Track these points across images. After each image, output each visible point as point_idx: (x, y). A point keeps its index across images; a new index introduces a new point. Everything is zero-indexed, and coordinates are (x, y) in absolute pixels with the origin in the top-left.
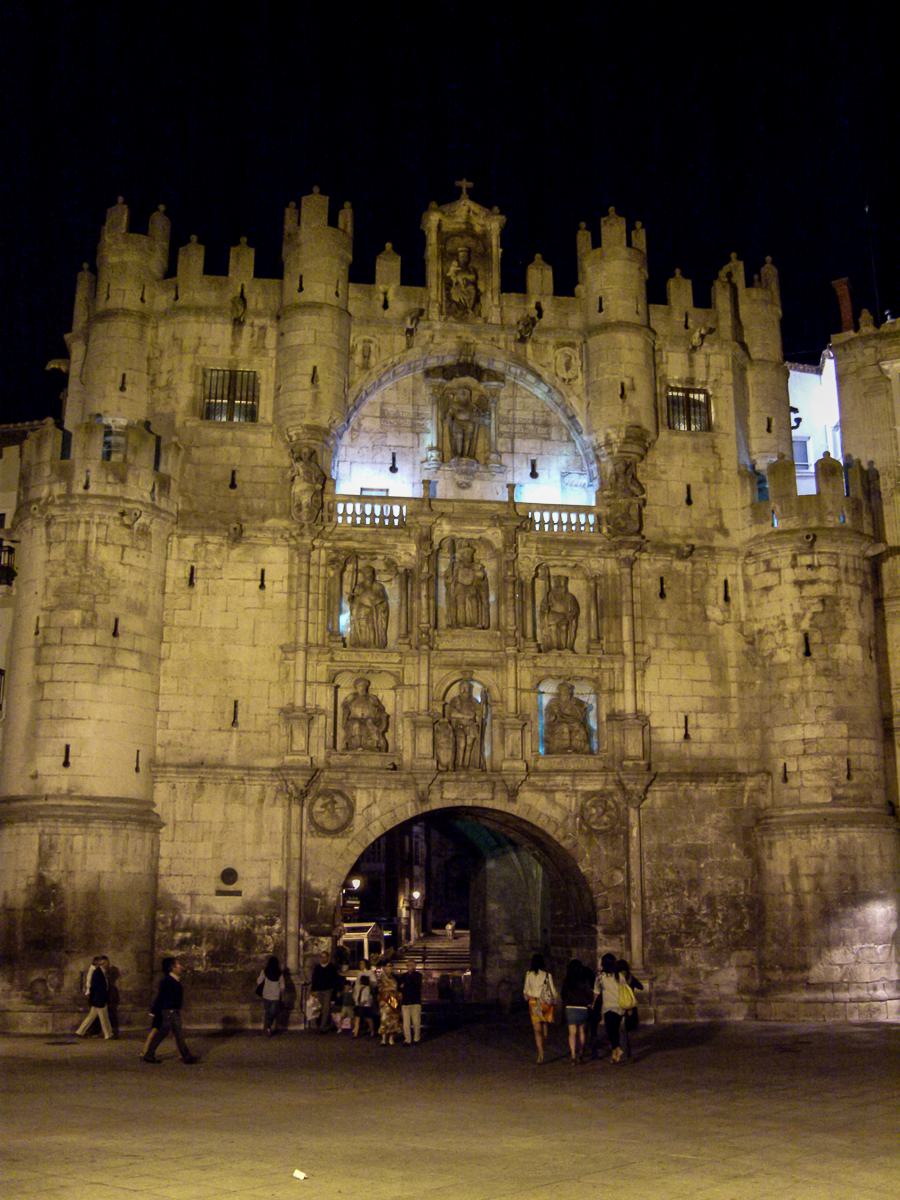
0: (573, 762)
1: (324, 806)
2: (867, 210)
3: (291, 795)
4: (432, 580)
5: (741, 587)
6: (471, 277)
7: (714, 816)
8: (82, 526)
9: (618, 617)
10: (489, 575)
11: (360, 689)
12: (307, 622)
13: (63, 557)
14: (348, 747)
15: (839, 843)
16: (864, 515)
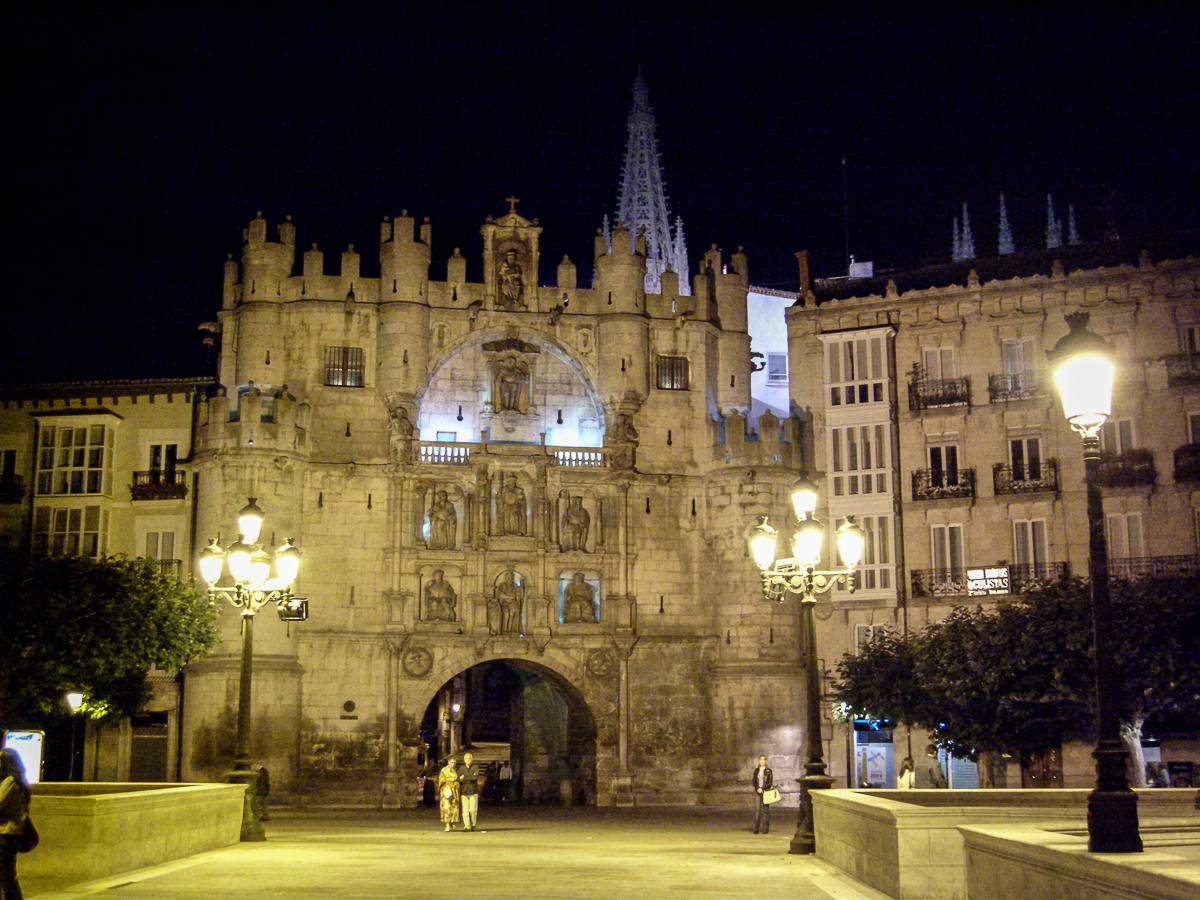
0: (582, 629)
2: (844, 162)
3: (391, 651)
4: (487, 502)
5: (704, 504)
6: (516, 276)
7: (679, 666)
8: (248, 469)
9: (616, 527)
10: (527, 495)
11: (437, 578)
12: (401, 531)
13: (236, 491)
14: (429, 619)
15: (761, 686)
16: (794, 455)
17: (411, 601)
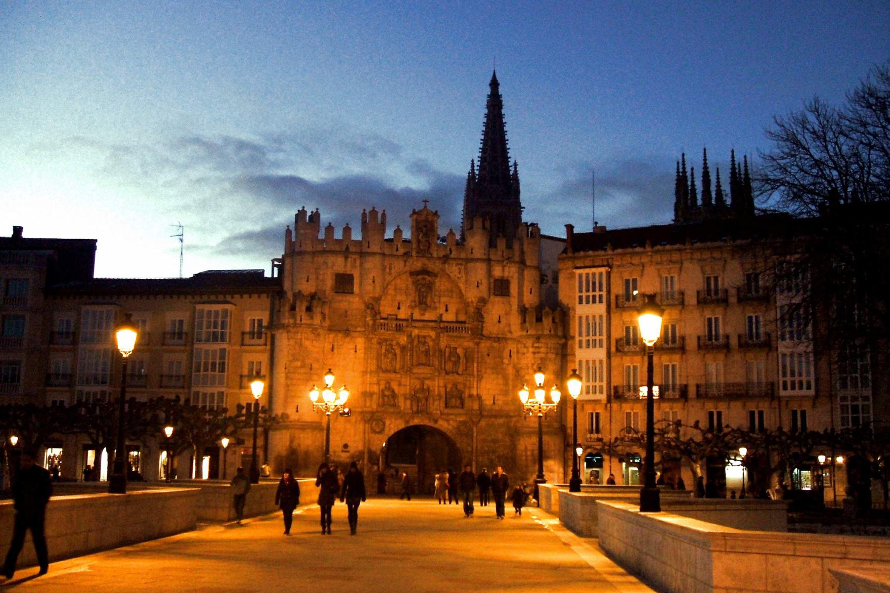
0: (456, 411)
1: (376, 424)
4: (412, 350)
5: (515, 352)
8: (300, 334)
9: (473, 362)
11: (387, 385)
17: (375, 397)
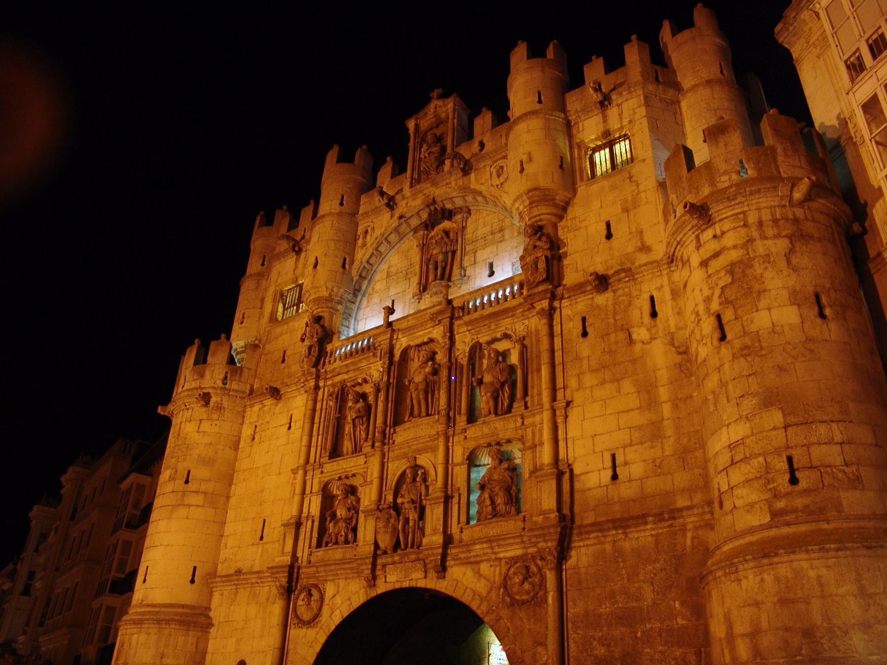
5: (668, 296)
15: (777, 579)
